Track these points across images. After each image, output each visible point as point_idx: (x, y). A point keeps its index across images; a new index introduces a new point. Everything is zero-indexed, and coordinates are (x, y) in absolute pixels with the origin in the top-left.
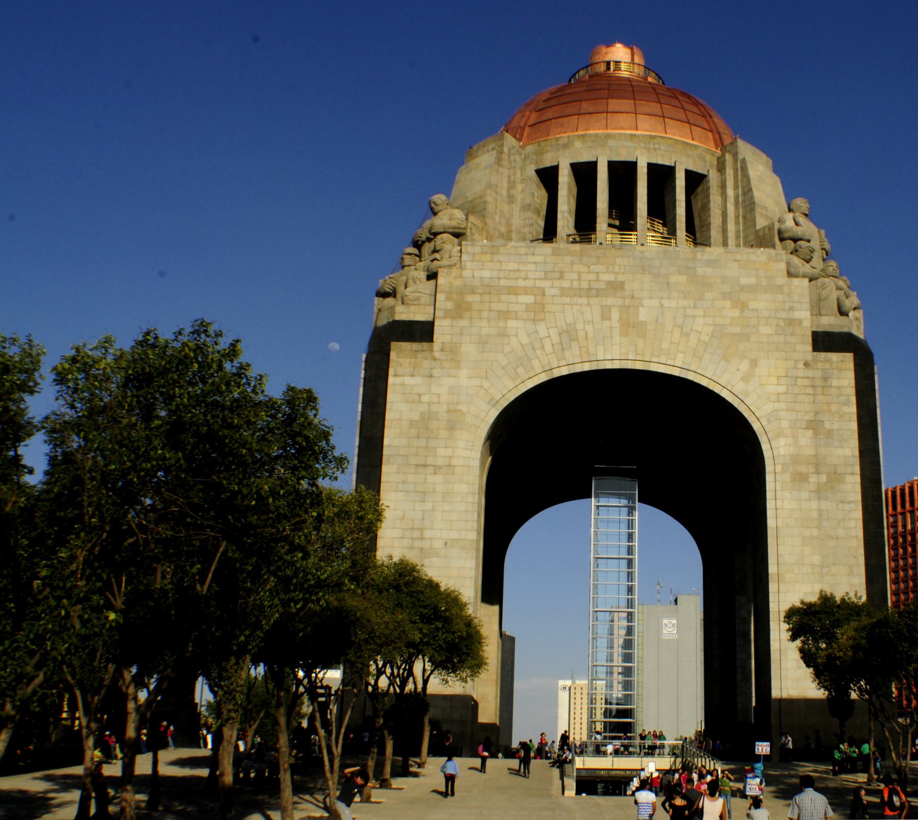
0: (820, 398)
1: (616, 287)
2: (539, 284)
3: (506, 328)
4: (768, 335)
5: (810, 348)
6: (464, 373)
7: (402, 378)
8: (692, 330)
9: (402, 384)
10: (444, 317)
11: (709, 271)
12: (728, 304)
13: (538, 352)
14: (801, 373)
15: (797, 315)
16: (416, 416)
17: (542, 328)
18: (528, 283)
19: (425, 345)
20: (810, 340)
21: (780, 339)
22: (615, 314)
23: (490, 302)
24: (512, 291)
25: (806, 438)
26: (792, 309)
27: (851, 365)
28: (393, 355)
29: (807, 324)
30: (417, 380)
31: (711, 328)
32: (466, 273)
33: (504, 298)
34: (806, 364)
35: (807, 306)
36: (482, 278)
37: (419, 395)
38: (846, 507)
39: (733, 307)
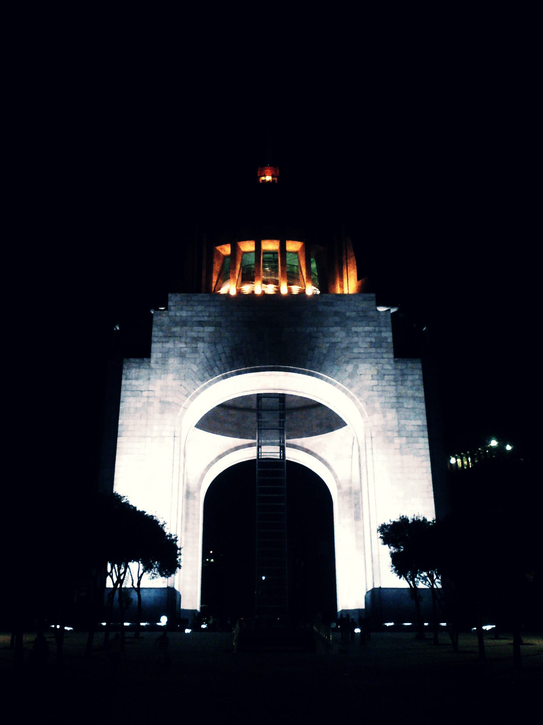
0: (401, 387)
3: (196, 348)
4: (366, 348)
5: (392, 356)
6: (170, 377)
7: (130, 381)
8: (316, 346)
9: (130, 385)
10: (159, 342)
13: (218, 363)
14: (387, 372)
15: (384, 334)
16: (139, 405)
17: (219, 347)
18: (210, 319)
21: (373, 350)
24: (201, 324)
25: (391, 415)
26: (381, 332)
29: (390, 340)
30: (140, 382)
31: (328, 345)
32: (171, 313)
33: (196, 329)
35: (390, 329)
36: (181, 316)
38: (420, 459)
39: (341, 330)
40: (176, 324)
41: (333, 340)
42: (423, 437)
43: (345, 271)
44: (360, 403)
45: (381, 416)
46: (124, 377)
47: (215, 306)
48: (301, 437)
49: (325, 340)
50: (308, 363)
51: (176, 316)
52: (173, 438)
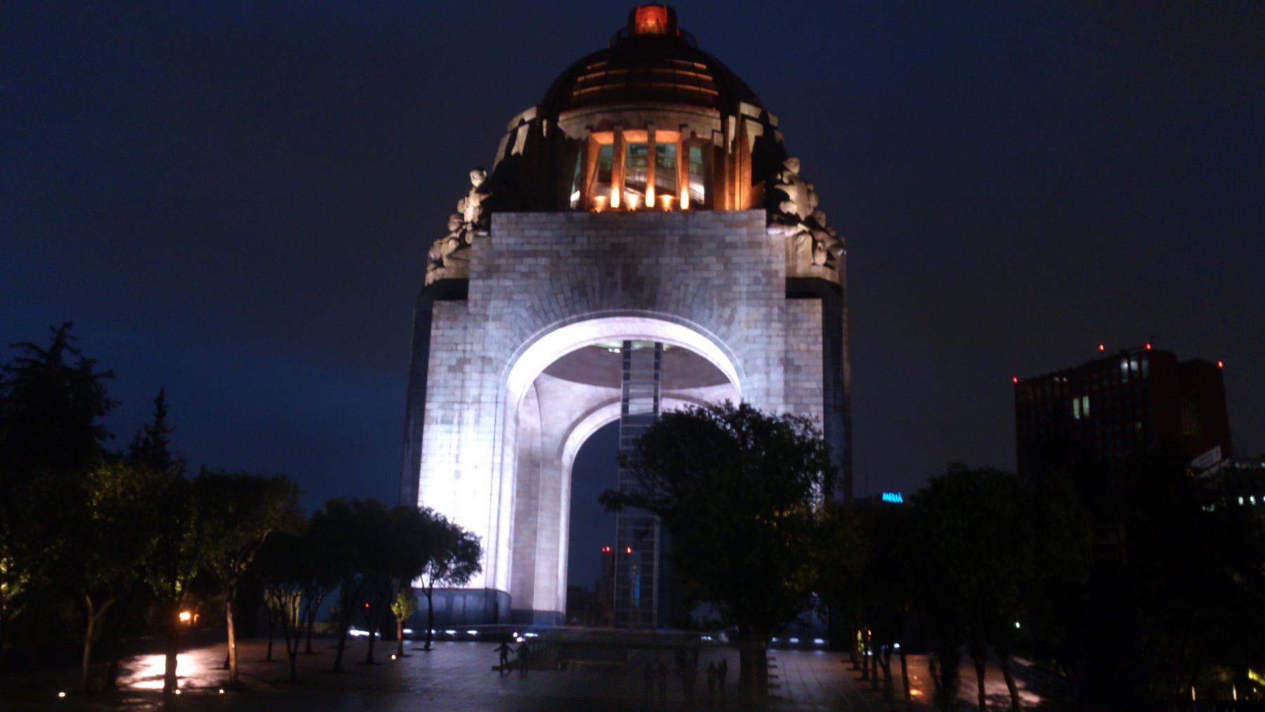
1: (618, 249)
2: (555, 248)
5: (783, 295)
10: (478, 278)
11: (699, 232)
12: (714, 260)
13: (554, 306)
15: (774, 267)
19: (461, 302)
20: (783, 288)
22: (619, 273)
23: (515, 265)
24: (534, 254)
27: (820, 308)
28: (435, 311)
29: (782, 275)
34: (781, 308)
36: (508, 244)
37: (456, 344)
40: (500, 255)
41: (706, 274)
42: (816, 404)
43: (737, 172)
44: (737, 360)
45: (763, 376)
46: (433, 325)
47: (552, 230)
48: (697, 386)
49: (698, 275)
50: (672, 307)
51: (501, 243)
52: (494, 404)
